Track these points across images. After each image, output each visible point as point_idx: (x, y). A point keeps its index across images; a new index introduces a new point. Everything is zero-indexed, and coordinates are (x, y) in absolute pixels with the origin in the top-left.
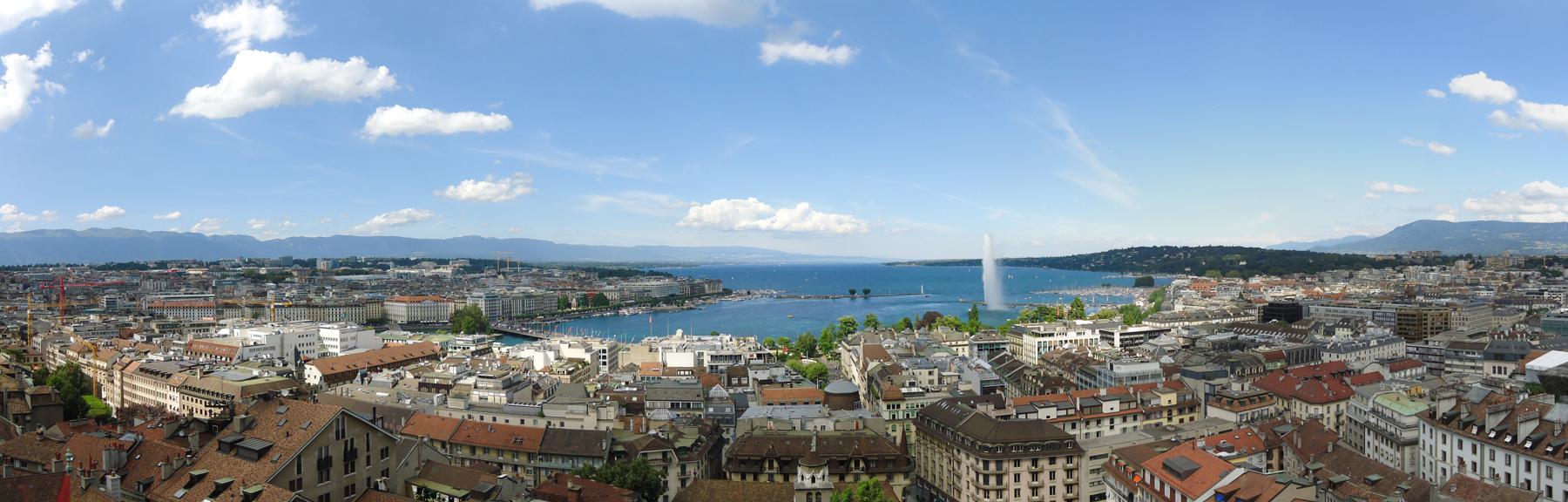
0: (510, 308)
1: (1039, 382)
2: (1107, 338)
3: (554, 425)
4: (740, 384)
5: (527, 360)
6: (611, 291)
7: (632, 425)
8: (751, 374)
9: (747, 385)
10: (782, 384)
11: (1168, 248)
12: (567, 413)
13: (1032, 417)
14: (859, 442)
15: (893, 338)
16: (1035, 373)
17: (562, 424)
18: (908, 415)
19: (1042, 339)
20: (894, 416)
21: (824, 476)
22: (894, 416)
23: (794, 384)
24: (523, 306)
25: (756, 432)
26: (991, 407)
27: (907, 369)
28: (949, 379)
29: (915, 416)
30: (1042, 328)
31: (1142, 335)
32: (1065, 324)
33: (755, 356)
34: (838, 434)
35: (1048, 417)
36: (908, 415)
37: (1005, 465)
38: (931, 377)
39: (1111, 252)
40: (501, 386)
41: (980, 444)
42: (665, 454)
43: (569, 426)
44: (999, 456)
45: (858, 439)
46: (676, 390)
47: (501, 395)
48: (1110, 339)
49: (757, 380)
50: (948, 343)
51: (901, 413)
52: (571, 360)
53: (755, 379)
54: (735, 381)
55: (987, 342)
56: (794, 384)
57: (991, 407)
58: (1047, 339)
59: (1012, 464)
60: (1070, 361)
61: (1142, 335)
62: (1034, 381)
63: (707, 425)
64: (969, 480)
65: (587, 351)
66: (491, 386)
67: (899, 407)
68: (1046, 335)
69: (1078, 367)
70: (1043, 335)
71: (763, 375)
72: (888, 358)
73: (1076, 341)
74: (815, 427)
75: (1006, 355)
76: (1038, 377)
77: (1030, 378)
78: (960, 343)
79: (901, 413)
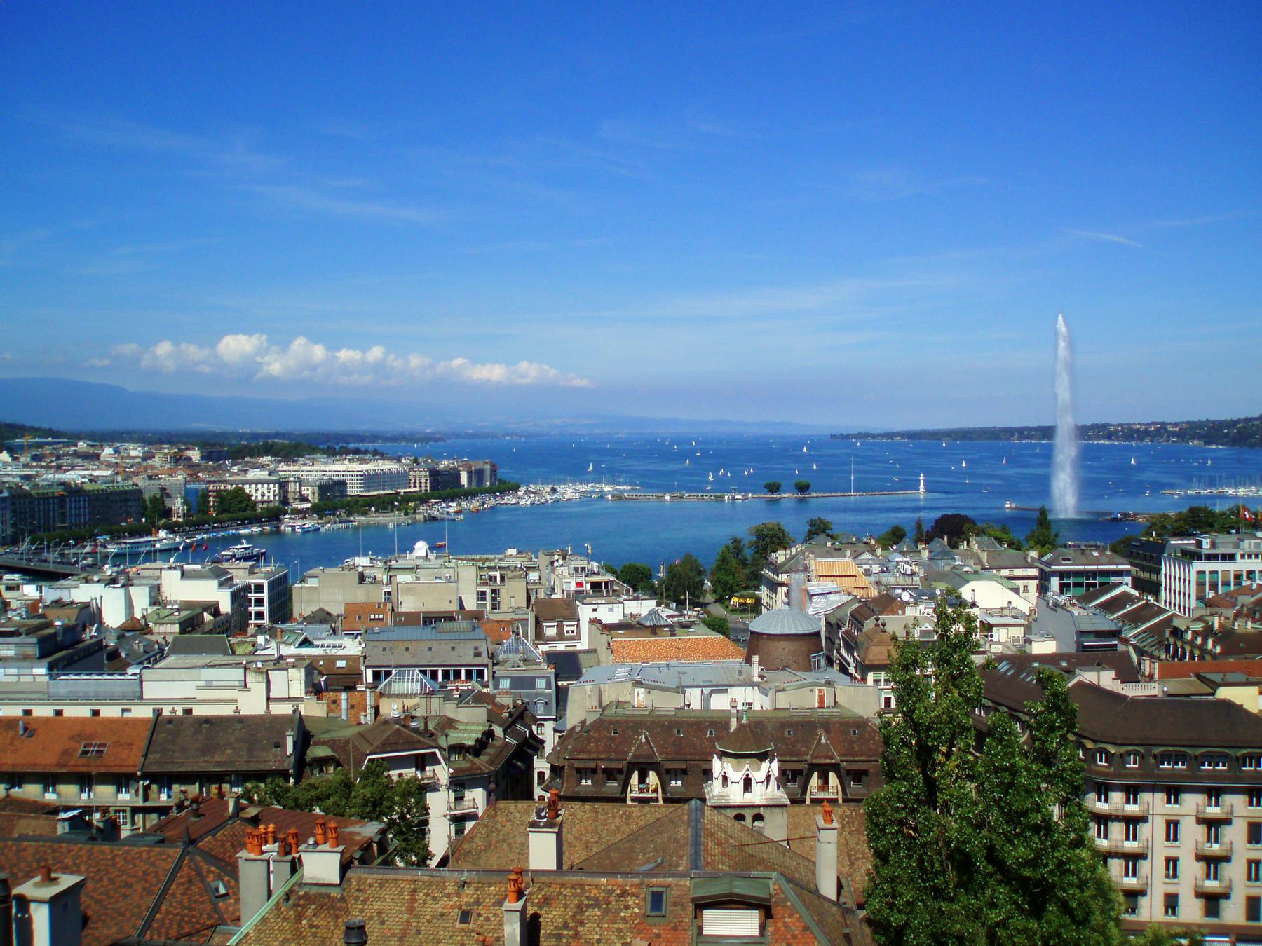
4: (561, 637)
5: (86, 606)
6: (262, 482)
8: (585, 612)
9: (577, 638)
12: (199, 688)
16: (1199, 627)
19: (1208, 566)
23: (678, 630)
25: (610, 713)
28: (1003, 631)
34: (781, 714)
40: (34, 651)
41: (1089, 745)
44: (1131, 774)
45: (826, 725)
46: (429, 644)
47: (36, 671)
49: (600, 622)
52: (188, 605)
53: (594, 622)
54: (550, 631)
56: (678, 630)
58: (1219, 566)
62: (1199, 641)
63: (502, 707)
65: (221, 585)
66: (11, 653)
70: (1209, 557)
71: (612, 614)
74: (734, 700)
76: (1208, 632)
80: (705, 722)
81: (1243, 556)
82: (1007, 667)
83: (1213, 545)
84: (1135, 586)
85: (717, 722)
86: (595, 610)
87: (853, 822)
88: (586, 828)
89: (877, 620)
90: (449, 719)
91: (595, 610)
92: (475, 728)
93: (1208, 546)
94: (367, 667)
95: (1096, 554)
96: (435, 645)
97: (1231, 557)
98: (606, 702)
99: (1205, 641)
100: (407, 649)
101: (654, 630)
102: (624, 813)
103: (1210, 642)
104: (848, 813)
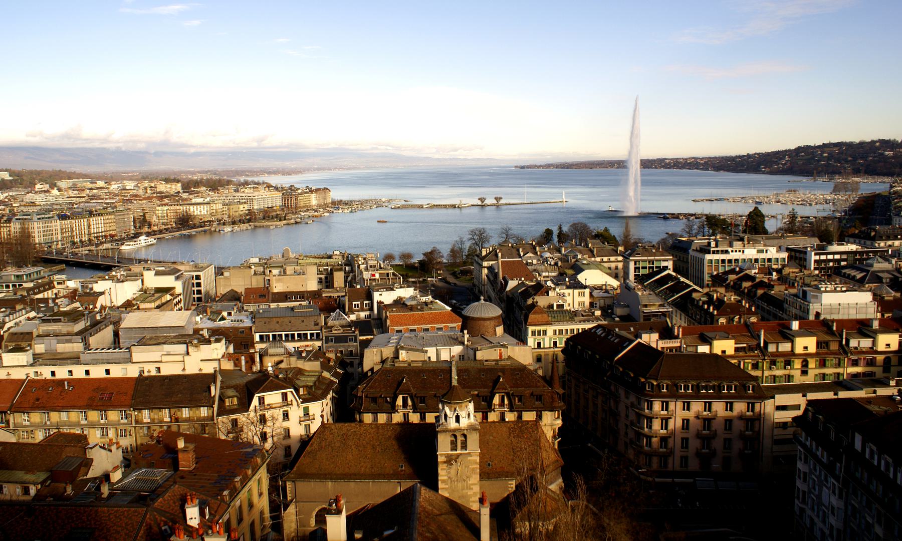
0: (72, 231)
1: (711, 308)
2: (796, 258)
3: (149, 371)
7: (243, 363)
10: (411, 308)
11: (883, 142)
13: (703, 349)
14: (504, 374)
15: (536, 253)
17: (159, 369)
18: (555, 343)
20: (539, 344)
21: (469, 415)
22: (539, 344)
24: (89, 226)
26: (655, 336)
27: (554, 289)
29: (563, 345)
30: (713, 244)
31: (844, 257)
32: (742, 240)
33: (377, 276)
35: (724, 352)
36: (555, 343)
37: (672, 406)
38: (582, 299)
39: (799, 150)
42: (285, 396)
43: (167, 370)
45: (503, 370)
46: (290, 319)
48: (800, 259)
50: (598, 259)
51: (547, 340)
55: (646, 258)
57: (655, 336)
59: (680, 404)
60: (746, 284)
61: (844, 257)
62: (706, 306)
63: (329, 360)
64: (628, 423)
65: (177, 278)
67: (545, 333)
68: (718, 251)
69: (760, 292)
70: (714, 252)
72: (530, 277)
73: (756, 260)
75: (669, 274)
77: (701, 303)
78: (612, 259)
79: (547, 340)
80: (438, 369)
81: (732, 251)
82: (601, 332)
83: (717, 246)
84: (674, 271)
85: (445, 370)
86: (381, 295)
87: (515, 431)
88: (373, 437)
89: (533, 299)
90: (300, 369)
91: (381, 295)
92: (314, 374)
93: (714, 246)
94: (255, 333)
95: (654, 251)
96: (293, 319)
97: (727, 252)
98: (384, 357)
99: (709, 308)
100: (278, 323)
101: (411, 308)
102: (393, 429)
103: (711, 308)
104: (513, 426)
